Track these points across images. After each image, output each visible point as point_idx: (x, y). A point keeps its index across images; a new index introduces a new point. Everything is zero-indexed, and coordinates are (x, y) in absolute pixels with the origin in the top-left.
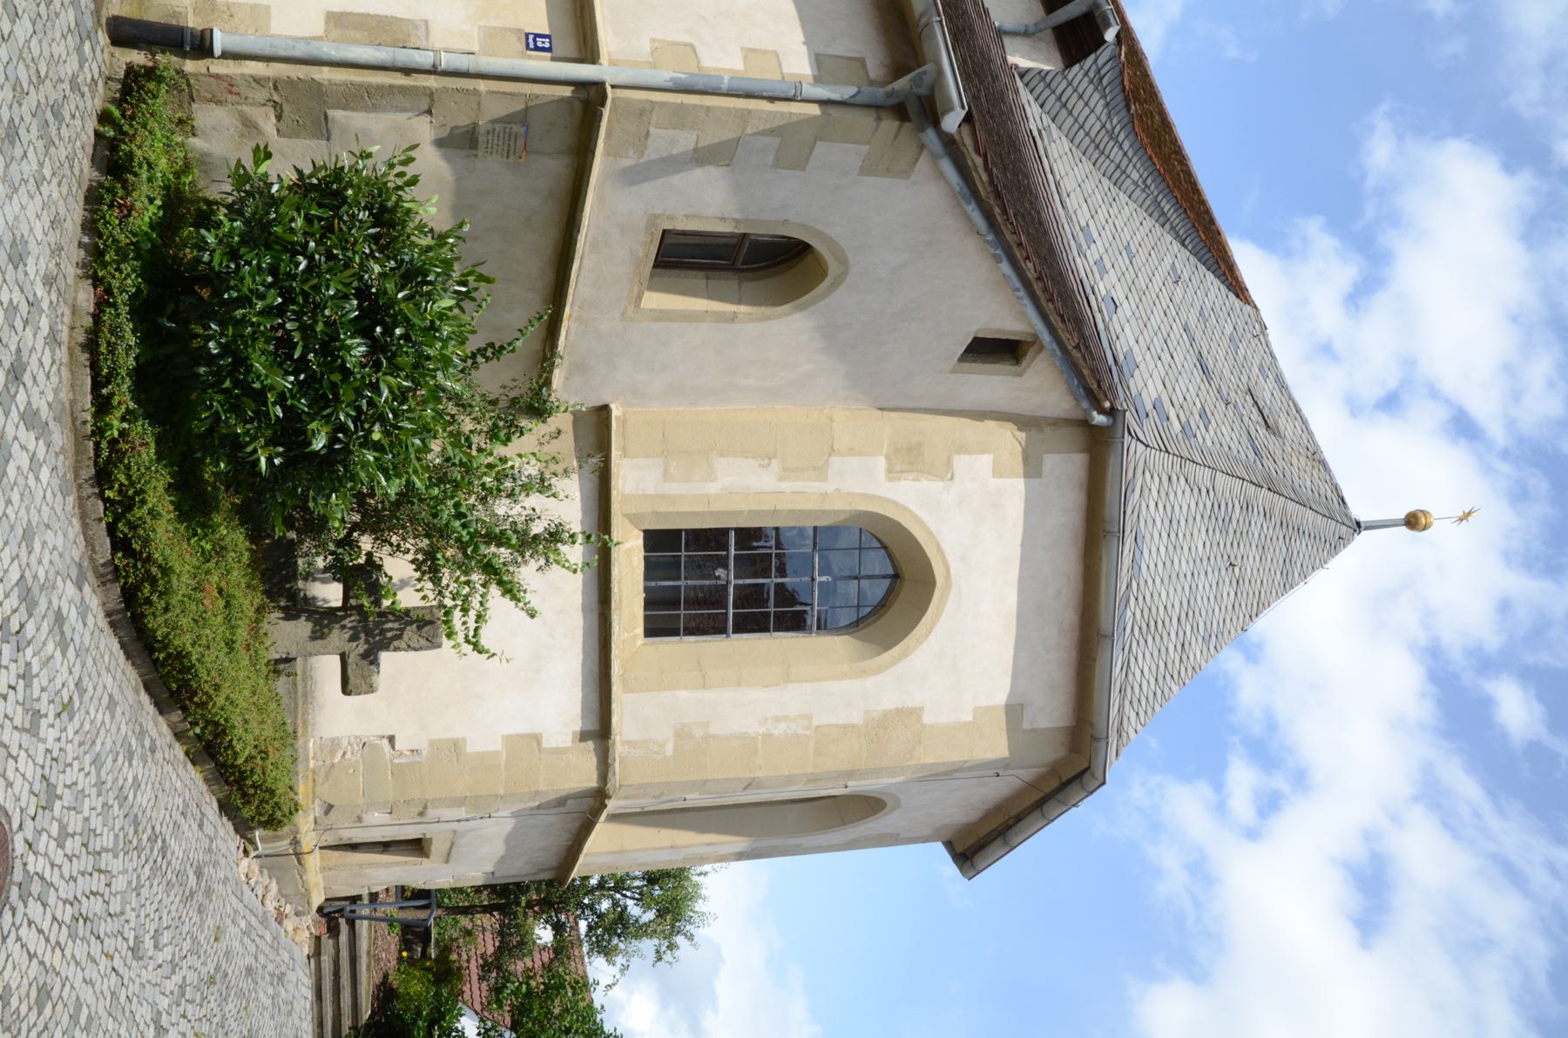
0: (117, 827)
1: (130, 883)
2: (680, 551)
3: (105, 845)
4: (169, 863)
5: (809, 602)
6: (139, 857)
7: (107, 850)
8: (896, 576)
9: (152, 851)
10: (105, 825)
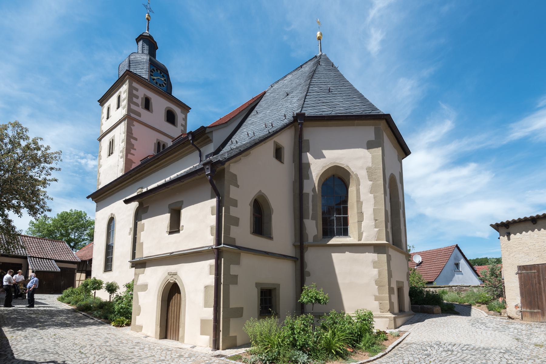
0: (397, 359)
1: (411, 356)
3: (402, 362)
4: (405, 347)
6: (404, 354)
7: (403, 362)
9: (402, 351)
10: (397, 362)
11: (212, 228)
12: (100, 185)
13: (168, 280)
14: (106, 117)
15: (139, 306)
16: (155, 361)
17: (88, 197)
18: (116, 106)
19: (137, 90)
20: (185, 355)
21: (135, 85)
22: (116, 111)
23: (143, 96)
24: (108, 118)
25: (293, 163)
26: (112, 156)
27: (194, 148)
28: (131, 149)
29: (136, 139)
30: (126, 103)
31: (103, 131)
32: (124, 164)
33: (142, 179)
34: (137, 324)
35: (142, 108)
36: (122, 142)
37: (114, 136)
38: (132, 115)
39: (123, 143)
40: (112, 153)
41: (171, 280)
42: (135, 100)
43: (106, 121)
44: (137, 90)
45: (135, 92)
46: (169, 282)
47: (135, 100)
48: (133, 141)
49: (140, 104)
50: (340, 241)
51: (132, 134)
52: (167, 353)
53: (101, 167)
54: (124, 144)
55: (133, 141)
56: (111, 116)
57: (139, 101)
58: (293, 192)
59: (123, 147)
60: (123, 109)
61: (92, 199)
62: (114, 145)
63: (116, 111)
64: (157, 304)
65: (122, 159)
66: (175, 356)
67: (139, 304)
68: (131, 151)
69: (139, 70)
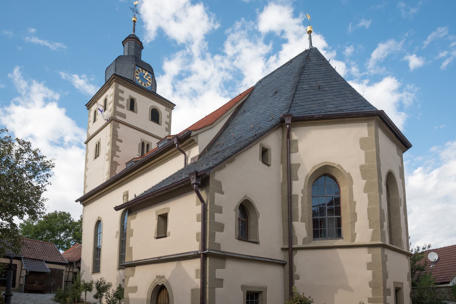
8: (325, 175)
11: (197, 234)
13: (157, 282)
14: (92, 120)
19: (123, 92)
21: (121, 87)
23: (128, 98)
26: (98, 159)
27: (179, 151)
28: (116, 151)
29: (121, 141)
30: (112, 106)
31: (89, 134)
32: (109, 166)
33: (127, 182)
35: (127, 109)
36: (108, 145)
37: (100, 139)
38: (118, 118)
39: (109, 145)
40: (98, 156)
41: (159, 283)
42: (120, 102)
43: (93, 124)
44: (123, 92)
45: (120, 94)
47: (120, 102)
48: (118, 143)
49: (125, 106)
51: (117, 136)
53: (88, 170)
54: (110, 147)
55: (118, 143)
56: (98, 119)
57: (124, 103)
59: (109, 150)
65: (108, 162)
68: (116, 153)
69: (125, 73)
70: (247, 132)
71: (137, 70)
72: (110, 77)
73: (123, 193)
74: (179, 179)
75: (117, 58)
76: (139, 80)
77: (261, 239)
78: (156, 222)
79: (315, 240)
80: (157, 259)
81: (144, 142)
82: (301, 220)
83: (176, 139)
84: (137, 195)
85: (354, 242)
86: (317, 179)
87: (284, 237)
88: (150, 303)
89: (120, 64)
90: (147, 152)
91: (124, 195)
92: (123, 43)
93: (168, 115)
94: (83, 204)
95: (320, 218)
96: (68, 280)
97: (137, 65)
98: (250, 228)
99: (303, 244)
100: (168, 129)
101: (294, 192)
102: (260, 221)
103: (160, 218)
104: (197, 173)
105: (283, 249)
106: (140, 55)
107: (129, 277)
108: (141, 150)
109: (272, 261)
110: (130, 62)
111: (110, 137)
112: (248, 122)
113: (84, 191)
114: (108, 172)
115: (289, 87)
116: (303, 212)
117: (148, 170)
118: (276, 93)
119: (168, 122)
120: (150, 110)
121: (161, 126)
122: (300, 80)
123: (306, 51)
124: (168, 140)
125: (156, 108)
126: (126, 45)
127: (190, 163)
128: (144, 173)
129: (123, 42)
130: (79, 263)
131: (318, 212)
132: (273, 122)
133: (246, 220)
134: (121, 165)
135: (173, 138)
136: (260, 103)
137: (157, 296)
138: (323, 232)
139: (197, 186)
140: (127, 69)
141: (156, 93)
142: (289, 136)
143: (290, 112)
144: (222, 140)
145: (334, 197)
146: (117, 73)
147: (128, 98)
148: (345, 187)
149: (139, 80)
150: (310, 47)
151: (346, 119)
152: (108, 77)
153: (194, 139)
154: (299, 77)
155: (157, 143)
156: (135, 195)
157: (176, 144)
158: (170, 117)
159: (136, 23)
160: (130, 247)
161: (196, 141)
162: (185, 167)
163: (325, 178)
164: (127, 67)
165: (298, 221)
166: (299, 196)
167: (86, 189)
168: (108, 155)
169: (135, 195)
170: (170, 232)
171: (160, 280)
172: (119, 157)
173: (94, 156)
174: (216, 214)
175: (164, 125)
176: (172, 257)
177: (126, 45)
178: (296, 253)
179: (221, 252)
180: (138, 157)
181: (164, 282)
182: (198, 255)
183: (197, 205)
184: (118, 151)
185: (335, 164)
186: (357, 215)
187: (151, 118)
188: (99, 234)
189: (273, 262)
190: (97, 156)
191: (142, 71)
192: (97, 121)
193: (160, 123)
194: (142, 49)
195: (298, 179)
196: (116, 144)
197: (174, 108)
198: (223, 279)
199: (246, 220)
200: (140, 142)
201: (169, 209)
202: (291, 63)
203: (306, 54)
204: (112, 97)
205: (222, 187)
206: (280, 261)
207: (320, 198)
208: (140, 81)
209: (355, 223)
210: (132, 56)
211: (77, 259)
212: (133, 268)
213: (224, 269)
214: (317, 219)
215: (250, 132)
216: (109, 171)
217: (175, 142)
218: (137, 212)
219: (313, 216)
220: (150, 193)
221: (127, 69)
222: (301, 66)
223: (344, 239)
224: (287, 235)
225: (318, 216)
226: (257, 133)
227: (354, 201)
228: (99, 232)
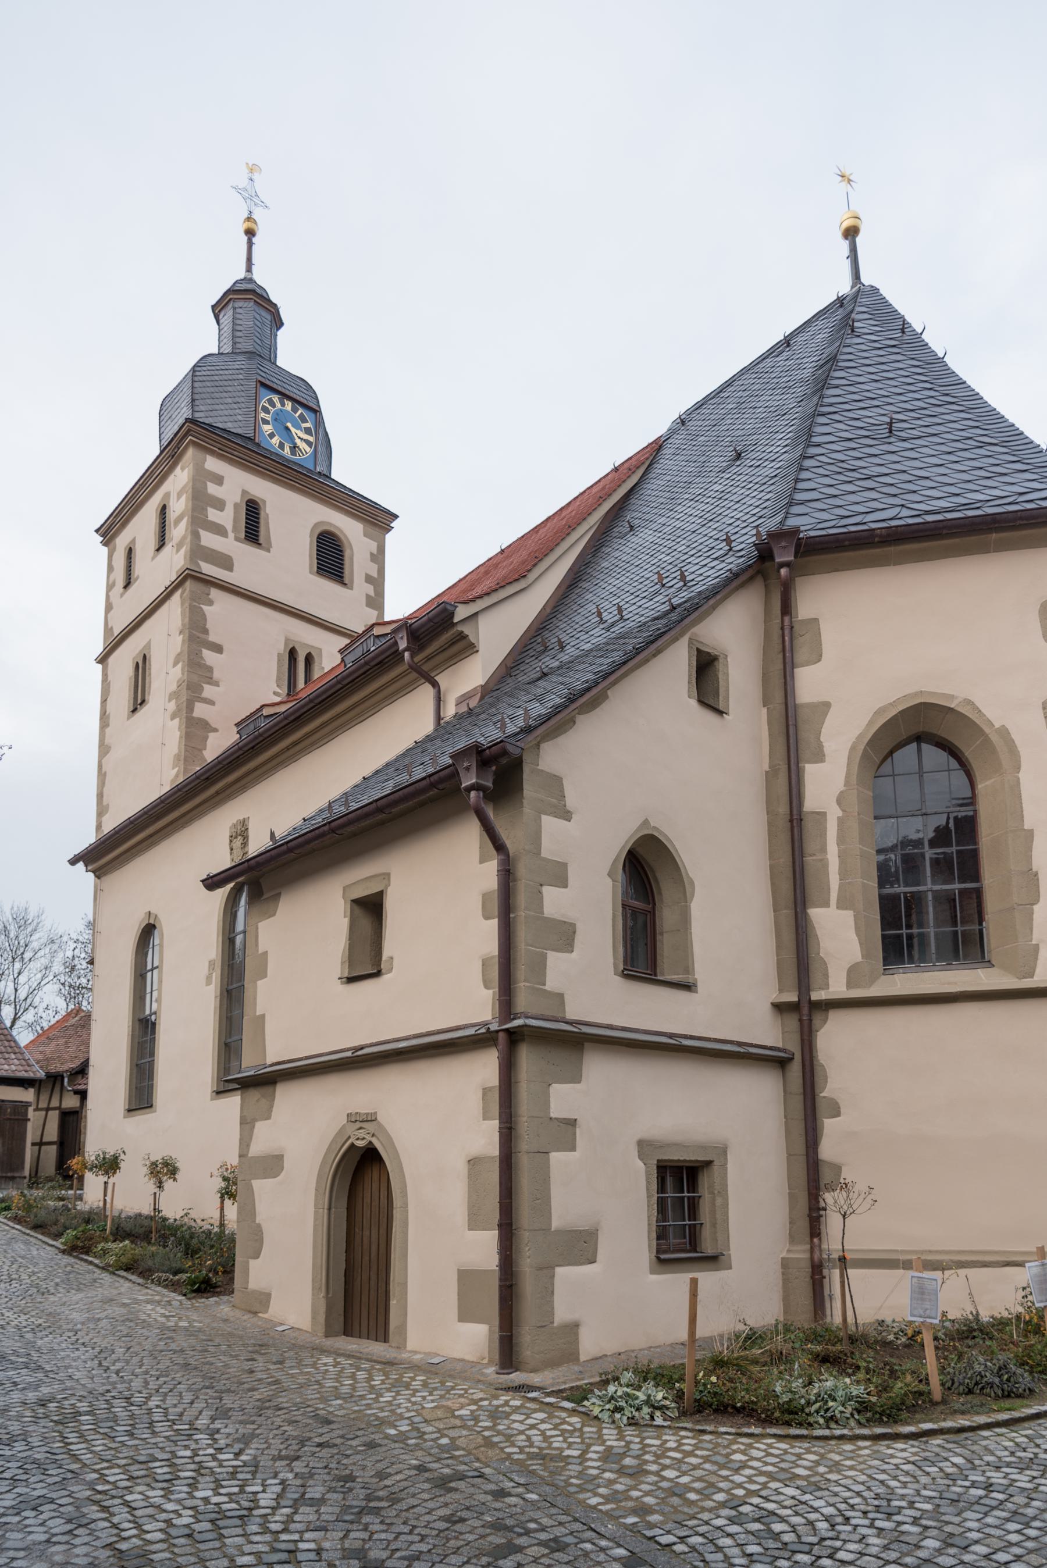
2: (902, 934)
5: (945, 815)
12: (107, 812)
13: (349, 1137)
15: (259, 1226)
16: (322, 1396)
17: (73, 862)
18: (152, 542)
19: (219, 480)
20: (413, 1383)
21: (213, 464)
22: (153, 559)
23: (238, 500)
24: (127, 585)
25: (764, 706)
28: (204, 685)
29: (218, 649)
32: (181, 737)
33: (244, 789)
34: (253, 1284)
35: (237, 539)
36: (175, 664)
37: (149, 643)
38: (208, 569)
39: (180, 665)
40: (143, 702)
41: (358, 1139)
42: (213, 515)
43: (122, 595)
44: (219, 480)
46: (352, 1145)
47: (213, 515)
48: (209, 656)
49: (229, 527)
50: (949, 983)
51: (206, 632)
52: (358, 1377)
53: (108, 752)
54: (182, 669)
55: (209, 656)
56: (138, 577)
57: (227, 517)
58: (768, 813)
59: (178, 682)
60: (178, 551)
61: (86, 866)
62: (150, 674)
63: (153, 559)
64: (316, 1219)
65: (177, 721)
66: (383, 1386)
67: (257, 1222)
69: (226, 412)
70: (645, 601)
71: (264, 402)
72: (176, 428)
73: (230, 828)
74: (419, 773)
75: (198, 362)
76: (272, 436)
77: (701, 973)
78: (345, 923)
79: (891, 972)
80: (349, 1054)
81: (296, 647)
82: (838, 900)
83: (404, 633)
84: (278, 835)
85: (1032, 977)
86: (891, 753)
87: (779, 964)
88: (326, 1211)
89: (208, 384)
90: (306, 683)
91: (234, 834)
92: (214, 311)
93: (375, 552)
94: (94, 872)
95: (905, 893)
96: (44, 1140)
97: (263, 384)
98: (662, 934)
99: (850, 985)
100: (376, 601)
101: (810, 804)
102: (696, 908)
103: (358, 910)
104: (477, 750)
105: (779, 1008)
106: (272, 349)
107: (254, 1121)
108: (287, 675)
109: (742, 1050)
110: (241, 377)
111: (182, 636)
112: (645, 563)
113: (99, 827)
114: (177, 757)
115: (784, 434)
116: (843, 873)
117: (313, 744)
118: (739, 456)
119: (375, 574)
120: (311, 535)
121: (352, 589)
122: (822, 406)
123: (840, 301)
124: (378, 637)
125: (332, 529)
126: (227, 317)
127: (454, 716)
128: (298, 757)
129: (213, 307)
130: (80, 1076)
131: (897, 871)
132: (733, 563)
133: (649, 907)
134: (220, 731)
135: (395, 631)
136: (686, 496)
137: (351, 1185)
138: (916, 941)
139: (481, 794)
140: (230, 400)
141: (330, 478)
142: (787, 609)
143: (792, 522)
144: (557, 630)
145: (952, 816)
146: (197, 415)
147: (238, 500)
148: (993, 780)
149: (272, 436)
150: (852, 287)
151: (990, 535)
152: (167, 430)
153: (466, 632)
154: (819, 394)
155: (341, 651)
156: (272, 834)
157: (406, 650)
158: (378, 557)
159: (254, 240)
160: (258, 1013)
161: (472, 639)
162: (436, 730)
163: (919, 750)
164: (230, 394)
165: (829, 906)
166: (829, 817)
167: (104, 819)
168: (177, 699)
169: (272, 834)
170: (392, 958)
171: (361, 1128)
172: (212, 703)
173: (129, 703)
174: (546, 890)
175: (361, 588)
176: (400, 1046)
177: (226, 317)
178: (825, 1021)
179: (567, 1023)
180: (278, 699)
181: (373, 1135)
182: (488, 1035)
183: (481, 863)
184: (209, 683)
185: (952, 697)
186: (1038, 879)
187: (318, 563)
188: (149, 971)
189: (744, 1053)
190: (141, 704)
191: (283, 405)
192: (137, 583)
193: (346, 580)
194: (278, 329)
195: (824, 755)
196: (202, 658)
197: (392, 525)
198: (576, 1120)
199: (649, 907)
200: (281, 648)
201: (387, 876)
202: (788, 346)
203: (841, 313)
204: (183, 498)
205: (566, 795)
206: (771, 1048)
207: (904, 819)
208: (276, 438)
209: (1033, 910)
210: (247, 352)
211: (75, 1064)
212: (267, 1090)
213: (579, 1082)
214: (896, 897)
215: (656, 600)
216: (180, 751)
217: (403, 645)
218: (279, 894)
219: (881, 884)
220: (324, 825)
221: (230, 400)
222: (824, 356)
223: (993, 966)
224: (790, 956)
225: (899, 887)
226: (676, 601)
227: (1026, 827)
228: (149, 967)
